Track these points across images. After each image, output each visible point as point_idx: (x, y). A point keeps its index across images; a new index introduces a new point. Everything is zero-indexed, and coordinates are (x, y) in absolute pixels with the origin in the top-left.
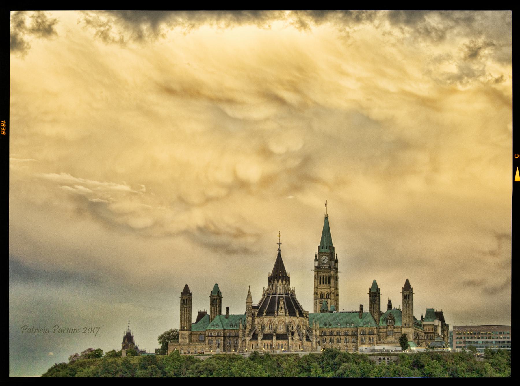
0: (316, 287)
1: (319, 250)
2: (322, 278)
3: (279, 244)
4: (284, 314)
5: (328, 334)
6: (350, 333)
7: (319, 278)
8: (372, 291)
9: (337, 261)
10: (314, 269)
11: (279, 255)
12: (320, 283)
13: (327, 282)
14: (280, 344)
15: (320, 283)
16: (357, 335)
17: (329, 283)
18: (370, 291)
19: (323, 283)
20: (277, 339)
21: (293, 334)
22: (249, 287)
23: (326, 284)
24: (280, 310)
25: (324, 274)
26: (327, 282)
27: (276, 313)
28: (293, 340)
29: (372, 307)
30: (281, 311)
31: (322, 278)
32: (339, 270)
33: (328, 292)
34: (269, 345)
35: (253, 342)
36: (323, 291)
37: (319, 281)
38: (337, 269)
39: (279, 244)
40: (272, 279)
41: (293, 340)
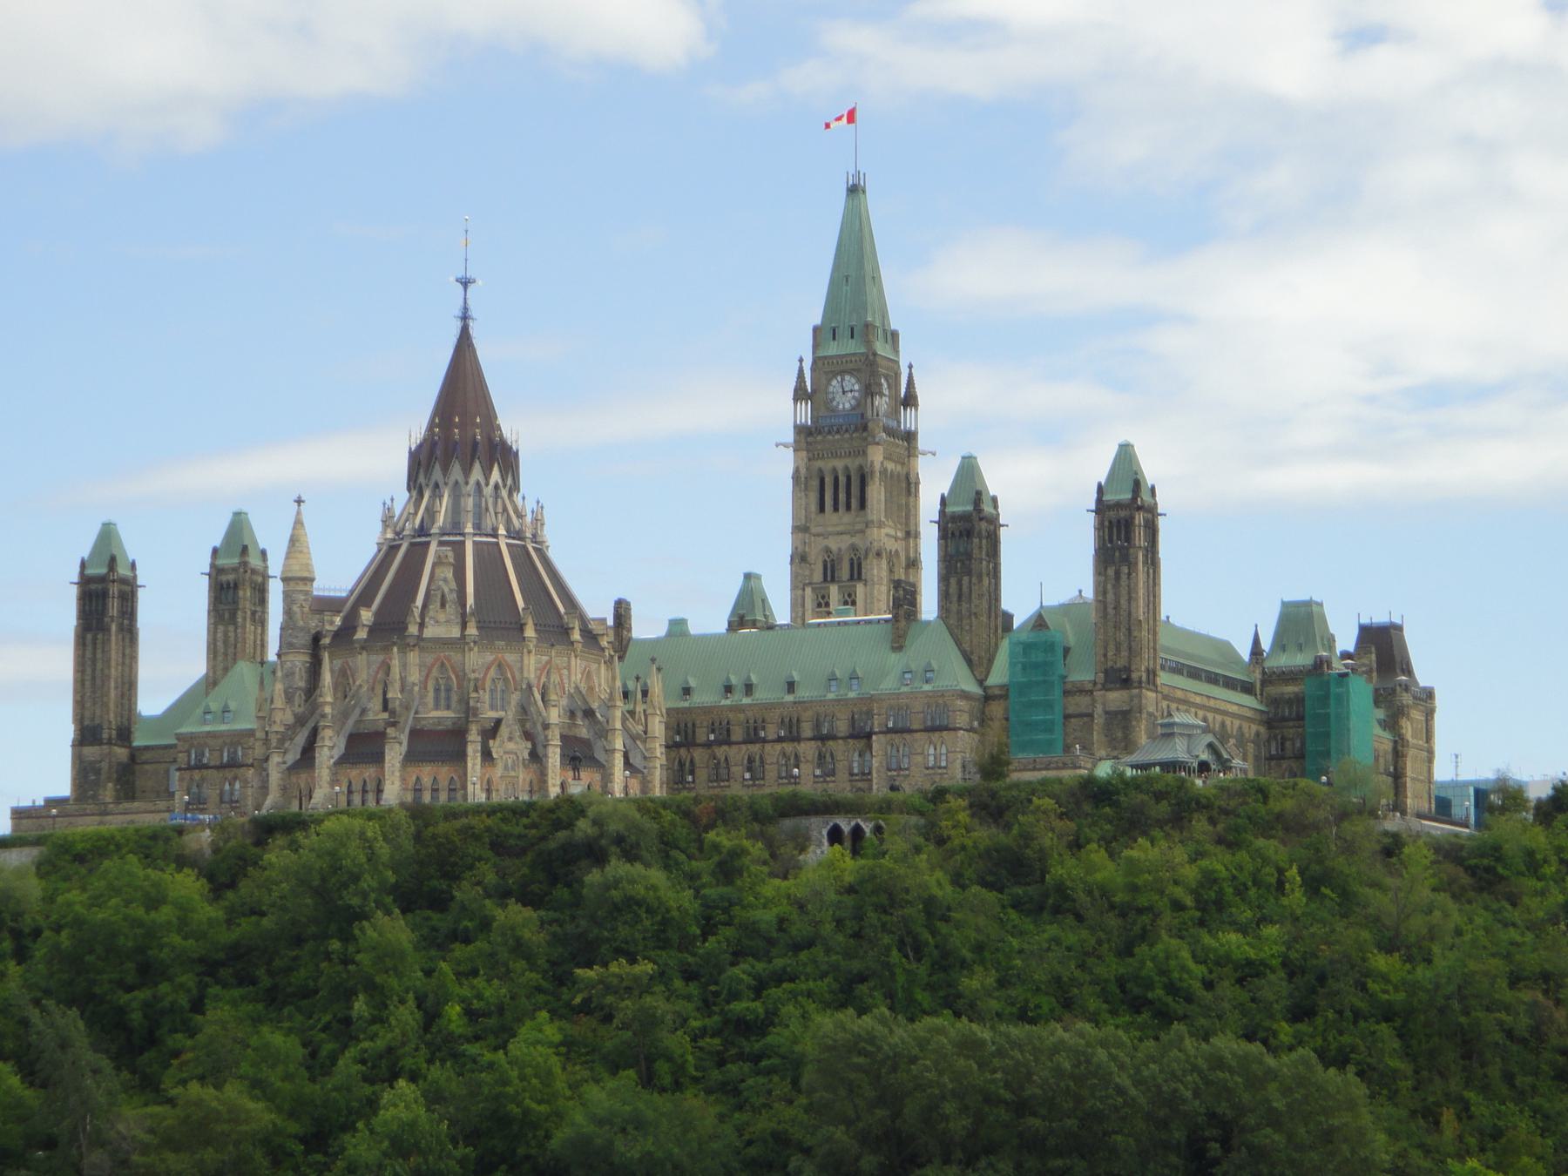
0: (800, 529)
1: (816, 346)
2: (829, 481)
3: (465, 283)
4: (455, 632)
5: (737, 734)
6: (842, 727)
7: (815, 483)
8: (949, 509)
9: (910, 400)
10: (789, 437)
11: (464, 345)
12: (822, 509)
13: (854, 503)
14: (427, 781)
15: (822, 509)
16: (869, 736)
17: (863, 504)
18: (942, 513)
19: (836, 509)
20: (411, 758)
21: (492, 731)
22: (299, 501)
23: (848, 507)
24: (434, 606)
25: (839, 464)
26: (854, 503)
27: (413, 629)
28: (487, 755)
29: (953, 589)
30: (442, 617)
31: (829, 481)
32: (922, 443)
33: (854, 548)
34: (371, 786)
35: (302, 779)
36: (833, 544)
37: (813, 497)
38: (910, 437)
39: (465, 283)
40: (427, 463)
41: (487, 755)
